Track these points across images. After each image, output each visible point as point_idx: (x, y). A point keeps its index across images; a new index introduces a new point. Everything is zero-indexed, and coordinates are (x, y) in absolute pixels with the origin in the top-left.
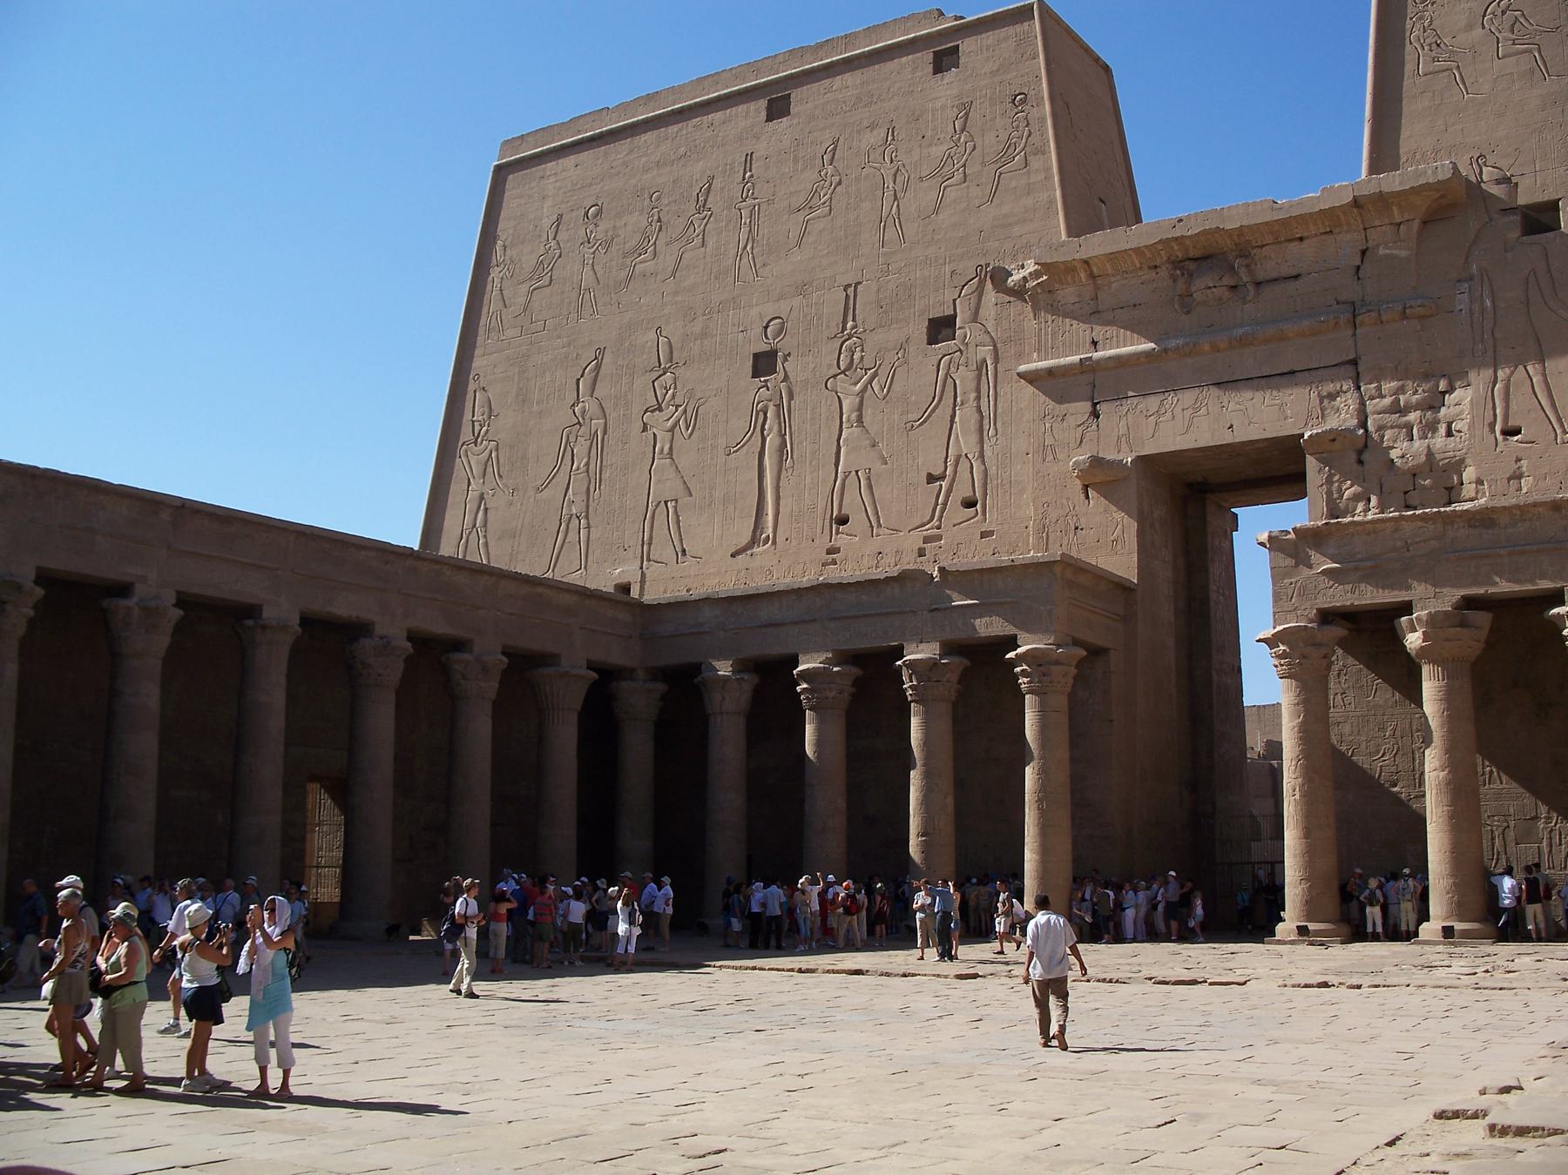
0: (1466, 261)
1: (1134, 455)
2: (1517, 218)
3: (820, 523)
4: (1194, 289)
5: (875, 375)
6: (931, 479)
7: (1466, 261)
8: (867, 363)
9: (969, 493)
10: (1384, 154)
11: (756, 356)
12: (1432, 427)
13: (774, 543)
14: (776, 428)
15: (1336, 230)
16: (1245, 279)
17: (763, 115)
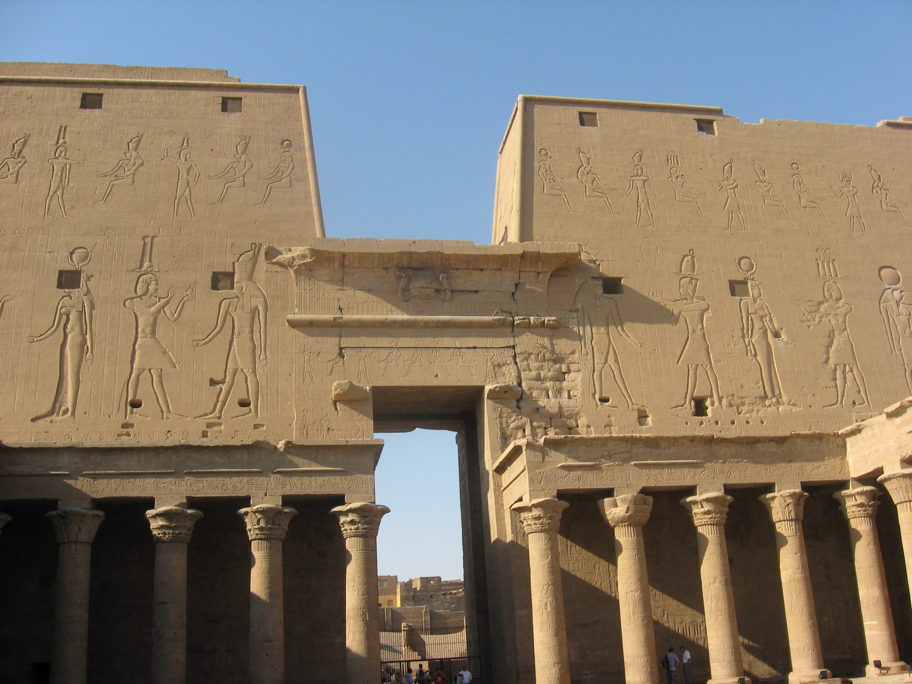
0: (575, 302)
1: (371, 385)
2: (601, 283)
3: (116, 404)
4: (411, 286)
5: (167, 303)
6: (213, 382)
7: (575, 302)
8: (160, 294)
9: (244, 396)
10: (525, 232)
11: (61, 273)
12: (559, 392)
13: (73, 414)
14: (77, 329)
15: (503, 269)
16: (446, 287)
17: (78, 103)
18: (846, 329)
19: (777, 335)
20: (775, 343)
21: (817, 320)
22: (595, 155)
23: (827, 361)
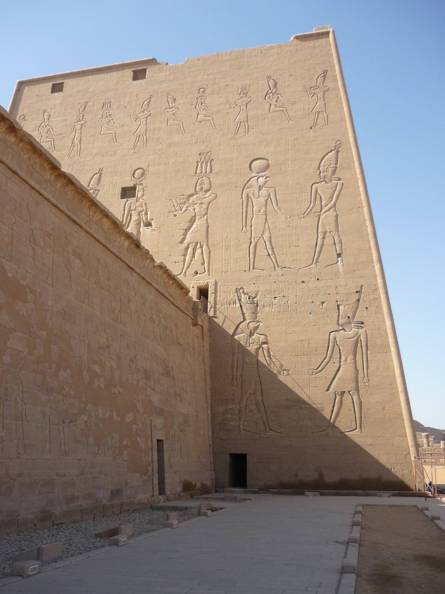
18: (206, 214)
19: (148, 224)
20: (144, 230)
21: (183, 209)
22: (54, 112)
23: (182, 242)
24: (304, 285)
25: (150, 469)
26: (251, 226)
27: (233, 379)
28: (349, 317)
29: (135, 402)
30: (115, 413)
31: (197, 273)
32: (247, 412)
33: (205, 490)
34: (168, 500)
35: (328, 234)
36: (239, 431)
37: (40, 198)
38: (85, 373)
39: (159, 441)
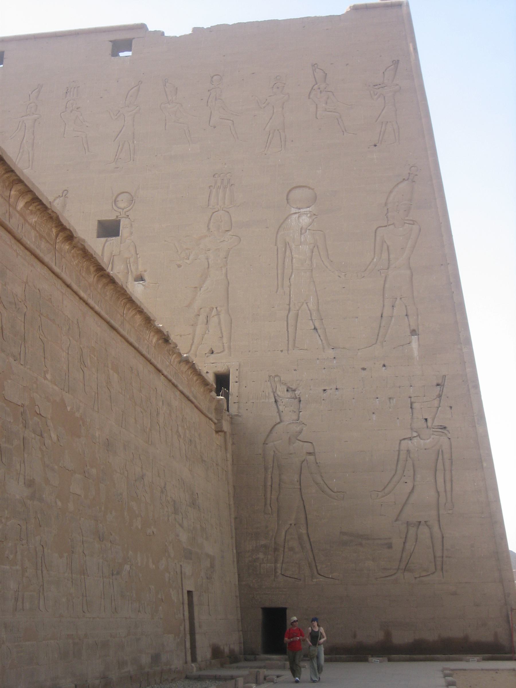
21: (191, 257)
24: (364, 373)
25: (182, 628)
26: (290, 286)
27: (266, 504)
28: (426, 420)
29: (166, 543)
30: (151, 560)
31: (213, 353)
32: (286, 550)
33: (233, 659)
34: (200, 669)
35: (398, 301)
36: (275, 576)
37: (86, 308)
38: (126, 513)
39: (190, 593)
